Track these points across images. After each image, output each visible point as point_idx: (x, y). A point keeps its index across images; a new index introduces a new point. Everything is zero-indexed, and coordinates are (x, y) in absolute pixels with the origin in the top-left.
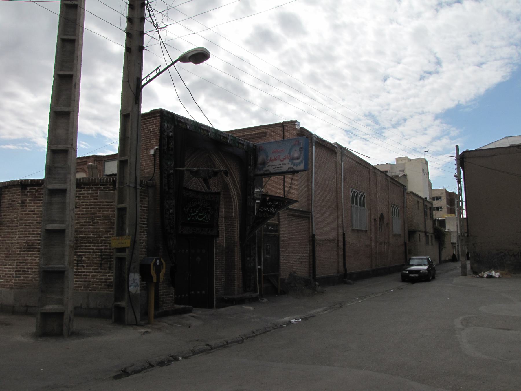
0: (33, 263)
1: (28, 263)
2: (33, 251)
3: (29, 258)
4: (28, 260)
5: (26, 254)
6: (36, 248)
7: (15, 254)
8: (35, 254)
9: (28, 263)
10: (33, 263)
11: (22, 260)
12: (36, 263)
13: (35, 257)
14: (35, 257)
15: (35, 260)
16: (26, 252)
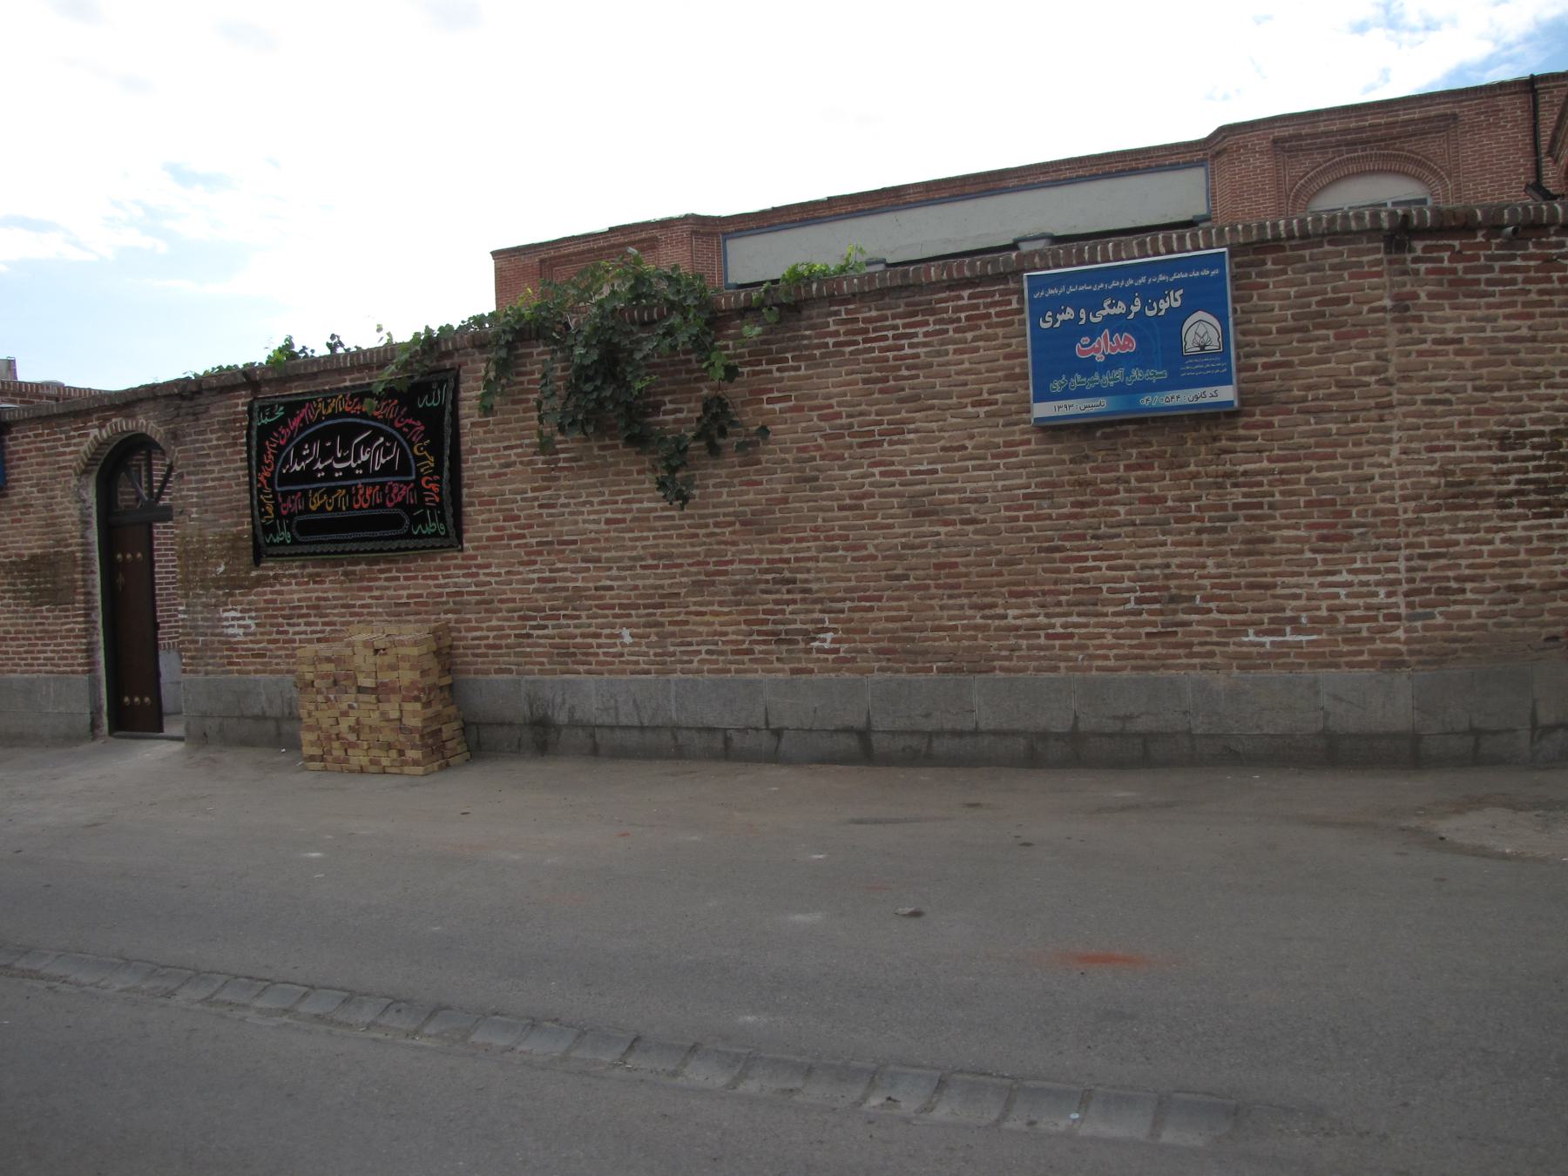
0: (1479, 554)
1: (1461, 556)
2: (1475, 507)
3: (1462, 537)
4: (1457, 543)
5: (1444, 520)
6: (1489, 494)
7: (1396, 523)
8: (1488, 518)
9: (1461, 556)
10: (1479, 554)
11: (1432, 544)
12: (1492, 554)
13: (1488, 530)
14: (1488, 530)
15: (1491, 542)
16: (1443, 514)
